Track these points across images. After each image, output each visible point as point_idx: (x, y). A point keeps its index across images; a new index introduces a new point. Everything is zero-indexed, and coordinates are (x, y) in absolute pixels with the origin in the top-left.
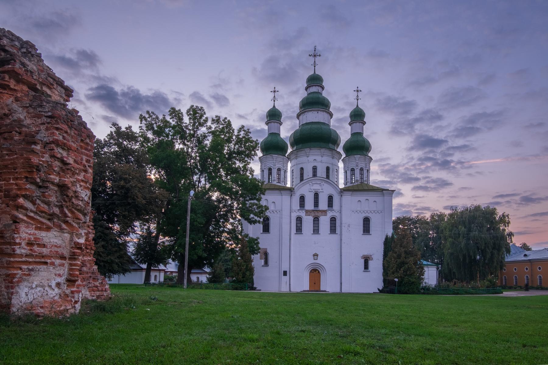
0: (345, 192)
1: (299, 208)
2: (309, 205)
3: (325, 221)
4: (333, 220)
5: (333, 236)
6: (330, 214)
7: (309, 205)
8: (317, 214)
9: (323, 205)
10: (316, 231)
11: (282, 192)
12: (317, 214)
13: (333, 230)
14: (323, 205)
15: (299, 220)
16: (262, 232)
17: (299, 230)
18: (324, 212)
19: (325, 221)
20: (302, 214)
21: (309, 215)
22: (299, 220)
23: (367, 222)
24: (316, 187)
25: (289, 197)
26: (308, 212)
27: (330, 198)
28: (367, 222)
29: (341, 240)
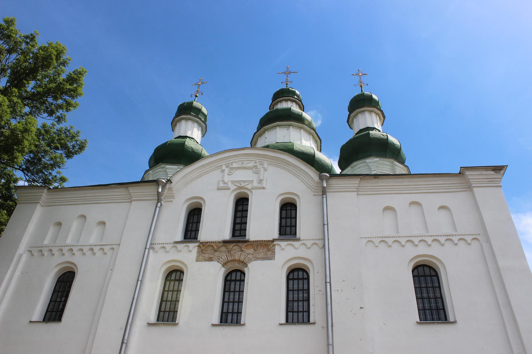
2: (216, 225)
3: (265, 284)
5: (298, 331)
6: (287, 254)
8: (237, 255)
10: (231, 312)
12: (237, 255)
15: (175, 276)
18: (266, 248)
19: (265, 284)
21: (210, 259)
22: (175, 276)
23: (427, 280)
24: (243, 176)
25: (149, 206)
26: (208, 251)
28: (427, 280)
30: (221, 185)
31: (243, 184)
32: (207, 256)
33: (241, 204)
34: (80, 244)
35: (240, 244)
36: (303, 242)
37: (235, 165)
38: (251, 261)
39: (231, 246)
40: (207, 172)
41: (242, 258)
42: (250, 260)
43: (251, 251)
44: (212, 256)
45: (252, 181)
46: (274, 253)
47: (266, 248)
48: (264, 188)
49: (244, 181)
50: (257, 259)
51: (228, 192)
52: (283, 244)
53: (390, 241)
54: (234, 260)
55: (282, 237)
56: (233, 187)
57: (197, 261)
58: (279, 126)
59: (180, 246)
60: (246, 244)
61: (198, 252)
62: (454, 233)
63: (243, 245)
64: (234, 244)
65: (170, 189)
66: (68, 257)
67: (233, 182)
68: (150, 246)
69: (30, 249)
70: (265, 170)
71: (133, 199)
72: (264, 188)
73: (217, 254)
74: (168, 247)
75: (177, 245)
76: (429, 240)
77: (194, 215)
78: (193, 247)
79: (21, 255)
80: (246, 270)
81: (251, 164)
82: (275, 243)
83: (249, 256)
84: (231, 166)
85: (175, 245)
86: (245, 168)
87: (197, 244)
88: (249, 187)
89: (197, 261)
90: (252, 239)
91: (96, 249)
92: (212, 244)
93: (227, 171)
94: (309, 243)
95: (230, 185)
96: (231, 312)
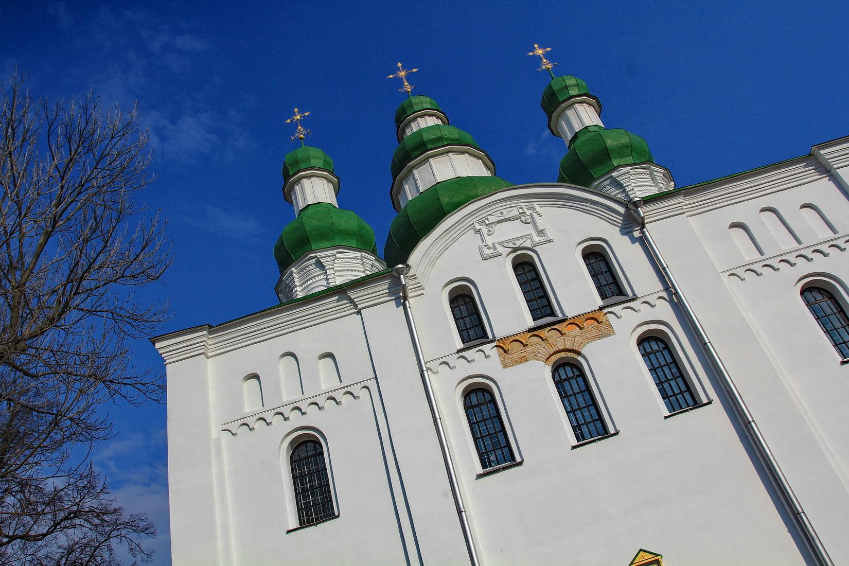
1: (460, 345)
2: (507, 310)
3: (618, 370)
6: (627, 323)
7: (507, 310)
9: (574, 291)
10: (589, 420)
11: (353, 294)
13: (679, 395)
14: (574, 291)
16: (293, 521)
17: (495, 447)
19: (618, 370)
20: (485, 363)
21: (524, 359)
25: (391, 309)
27: (597, 258)
30: (487, 252)
31: (518, 244)
32: (516, 356)
33: (527, 270)
34: (307, 395)
35: (556, 327)
36: (642, 300)
37: (492, 219)
38: (584, 345)
39: (544, 333)
40: (455, 240)
41: (569, 346)
44: (523, 354)
45: (529, 236)
46: (609, 325)
48: (550, 241)
49: (518, 239)
50: (590, 340)
52: (617, 309)
53: (757, 267)
54: (557, 352)
55: (610, 301)
57: (505, 366)
58: (433, 156)
59: (468, 354)
60: (565, 324)
61: (500, 355)
62: (836, 236)
64: (549, 328)
65: (414, 277)
66: (296, 420)
67: (501, 243)
69: (227, 427)
71: (359, 306)
72: (550, 241)
73: (529, 349)
74: (452, 360)
75: (463, 354)
76: (808, 253)
77: (465, 305)
78: (487, 348)
79: (218, 440)
80: (580, 358)
81: (515, 212)
82: (605, 311)
83: (577, 339)
84: (487, 222)
85: (460, 354)
86: (509, 220)
87: (494, 344)
88: (528, 244)
89: (505, 366)
90: (570, 314)
91: (338, 395)
92: (516, 338)
93: (485, 230)
94: (652, 299)
95: (500, 249)
96: (589, 420)
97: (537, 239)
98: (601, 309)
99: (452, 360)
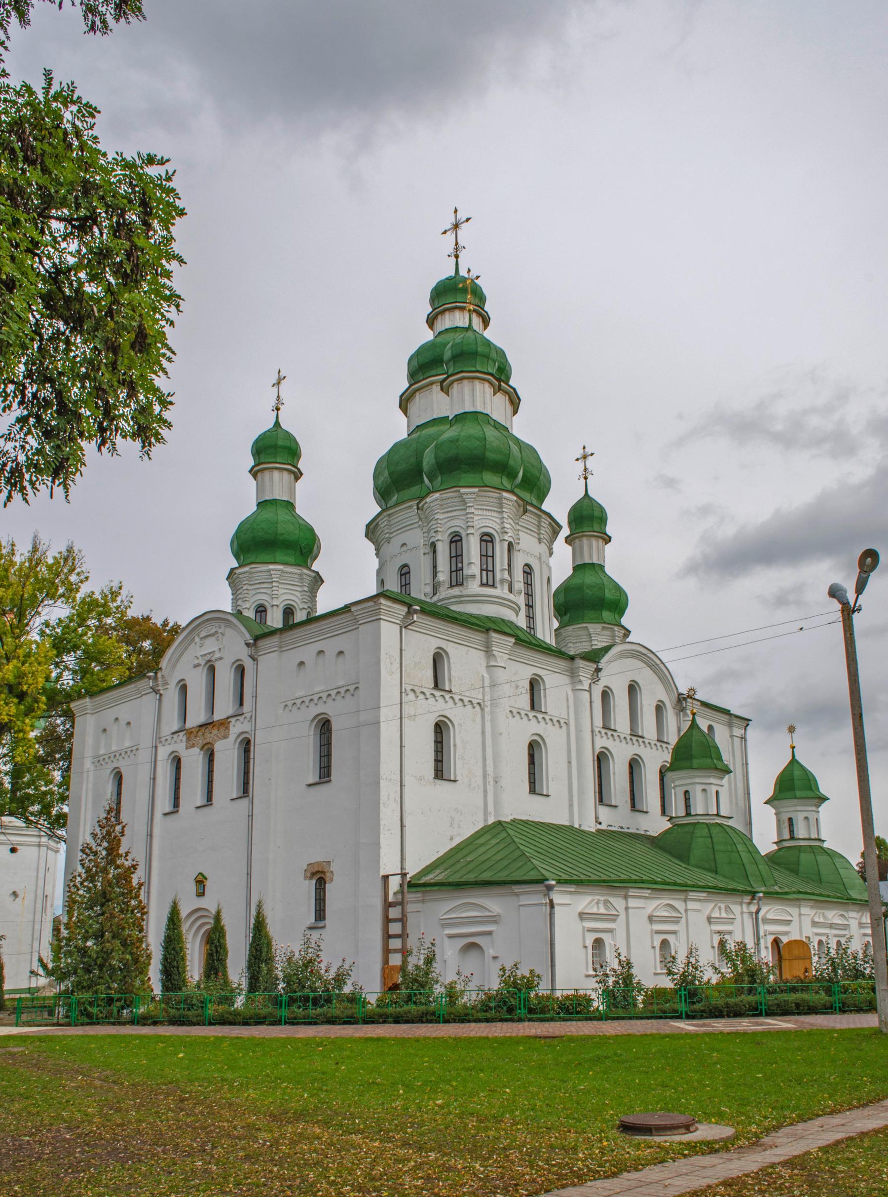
0: (261, 643)
4: (246, 746)
12: (209, 737)
22: (177, 762)
29: (251, 816)
37: (203, 634)
39: (203, 729)
42: (216, 741)
43: (215, 732)
45: (214, 652)
47: (224, 724)
49: (209, 653)
51: (200, 668)
56: (203, 662)
63: (210, 727)
67: (202, 656)
68: (158, 740)
70: (223, 634)
72: (221, 658)
81: (212, 631)
97: (217, 655)
98: (228, 718)
99: (169, 738)
